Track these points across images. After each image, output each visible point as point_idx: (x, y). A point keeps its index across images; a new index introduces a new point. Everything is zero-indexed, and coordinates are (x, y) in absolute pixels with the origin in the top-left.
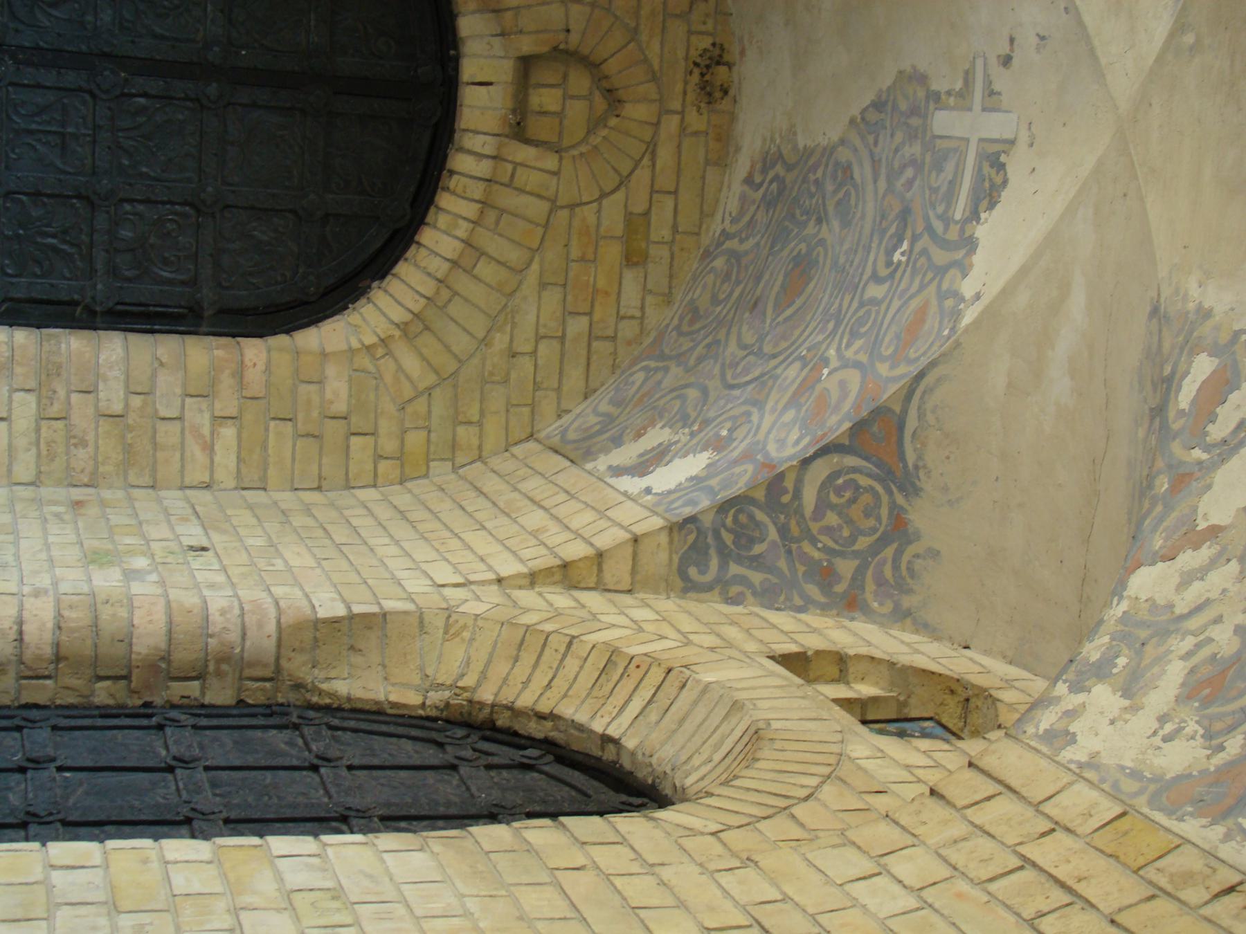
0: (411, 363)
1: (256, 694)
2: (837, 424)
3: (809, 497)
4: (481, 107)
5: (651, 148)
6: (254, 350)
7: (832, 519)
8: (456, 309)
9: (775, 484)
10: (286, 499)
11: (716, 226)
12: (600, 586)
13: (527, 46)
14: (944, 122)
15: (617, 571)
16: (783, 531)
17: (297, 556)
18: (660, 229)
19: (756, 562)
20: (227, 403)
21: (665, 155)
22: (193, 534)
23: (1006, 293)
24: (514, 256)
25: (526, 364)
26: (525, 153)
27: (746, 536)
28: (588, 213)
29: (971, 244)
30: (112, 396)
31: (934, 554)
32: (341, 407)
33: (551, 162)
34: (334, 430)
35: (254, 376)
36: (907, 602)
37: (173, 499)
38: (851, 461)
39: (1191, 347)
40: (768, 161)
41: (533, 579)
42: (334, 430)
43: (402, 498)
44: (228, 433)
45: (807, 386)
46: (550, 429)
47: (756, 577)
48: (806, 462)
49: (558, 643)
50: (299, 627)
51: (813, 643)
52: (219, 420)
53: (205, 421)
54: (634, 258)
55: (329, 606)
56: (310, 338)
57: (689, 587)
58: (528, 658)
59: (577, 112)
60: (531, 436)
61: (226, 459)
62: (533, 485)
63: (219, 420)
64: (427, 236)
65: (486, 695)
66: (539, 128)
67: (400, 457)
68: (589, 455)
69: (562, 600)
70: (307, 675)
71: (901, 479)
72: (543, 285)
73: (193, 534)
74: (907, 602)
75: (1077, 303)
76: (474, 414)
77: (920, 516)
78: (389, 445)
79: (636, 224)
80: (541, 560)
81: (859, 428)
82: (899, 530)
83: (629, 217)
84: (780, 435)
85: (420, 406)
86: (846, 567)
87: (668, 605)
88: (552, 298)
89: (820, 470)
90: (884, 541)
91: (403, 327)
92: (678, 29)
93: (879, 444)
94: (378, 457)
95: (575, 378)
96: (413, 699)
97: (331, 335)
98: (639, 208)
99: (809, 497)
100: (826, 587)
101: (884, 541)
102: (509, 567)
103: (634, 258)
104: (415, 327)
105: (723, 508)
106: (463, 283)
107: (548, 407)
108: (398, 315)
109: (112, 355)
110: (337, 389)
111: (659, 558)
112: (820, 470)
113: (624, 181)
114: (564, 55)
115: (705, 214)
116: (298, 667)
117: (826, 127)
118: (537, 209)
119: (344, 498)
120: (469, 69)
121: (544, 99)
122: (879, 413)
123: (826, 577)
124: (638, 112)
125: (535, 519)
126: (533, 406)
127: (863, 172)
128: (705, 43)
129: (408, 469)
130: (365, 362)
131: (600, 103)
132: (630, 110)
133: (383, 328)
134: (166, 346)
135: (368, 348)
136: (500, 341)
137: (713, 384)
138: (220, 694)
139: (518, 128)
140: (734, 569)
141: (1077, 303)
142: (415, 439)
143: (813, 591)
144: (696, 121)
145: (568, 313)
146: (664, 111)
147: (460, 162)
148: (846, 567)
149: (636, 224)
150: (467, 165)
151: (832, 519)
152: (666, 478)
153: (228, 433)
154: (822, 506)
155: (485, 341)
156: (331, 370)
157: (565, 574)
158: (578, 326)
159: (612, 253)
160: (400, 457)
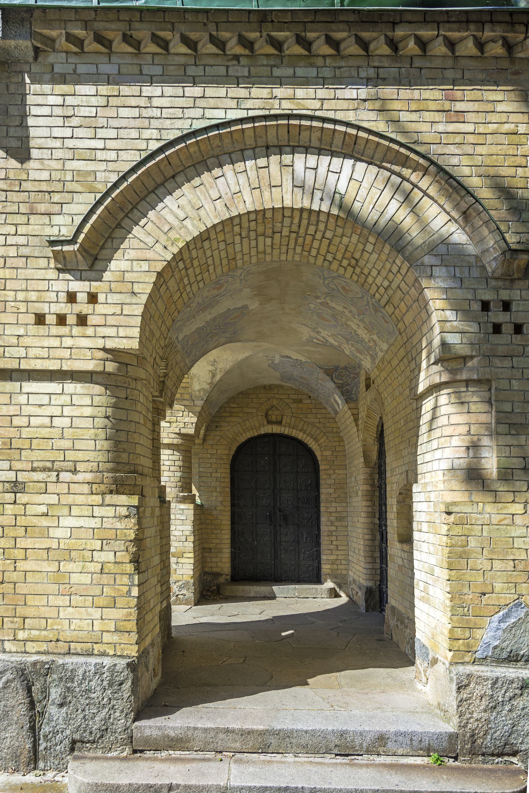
0: (322, 440)
1: (377, 471)
2: (328, 378)
3: (340, 382)
4: (276, 429)
5: (281, 399)
6: (322, 467)
7: (344, 378)
8: (312, 433)
9: (338, 387)
10: (347, 462)
11: (294, 386)
12: (358, 414)
13: (265, 422)
14: (277, 361)
15: (355, 412)
16: (347, 385)
17: (356, 462)
18: (296, 397)
19: (352, 389)
20: (331, 472)
21: (282, 397)
22: (353, 478)
23: (304, 356)
24: (302, 423)
25: (321, 420)
26: (284, 422)
27: (348, 391)
28: (293, 410)
29: (296, 359)
30: (331, 491)
31: (348, 363)
32: (331, 452)
33: (285, 417)
34: (335, 454)
35: (327, 467)
36: (357, 366)
37: (348, 481)
38: (334, 376)
39: (312, 341)
40: (282, 381)
41: (357, 425)
42: (335, 454)
43: (346, 442)
44: (336, 471)
45: (322, 380)
46: (333, 415)
47: (355, 389)
48: (335, 383)
49: (366, 424)
50: (365, 464)
51: (364, 383)
52: (334, 473)
53: (335, 475)
54: (300, 401)
55: (362, 460)
56: (319, 458)
57: (357, 400)
58: (369, 429)
59: (276, 412)
60: (334, 418)
61: (341, 472)
62: (343, 420)
63: (334, 473)
64: (299, 438)
65: (375, 435)
66: (279, 418)
67: (339, 441)
68: (337, 411)
69: (360, 422)
70: (373, 463)
71: (336, 368)
72: (307, 418)
73: (353, 478)
74: (357, 366)
75: (306, 348)
76: (331, 429)
77: (342, 365)
78: (337, 444)
79: (295, 401)
80: (353, 424)
81: (328, 375)
82: (345, 368)
83: (294, 403)
84: (331, 385)
85: (330, 438)
86: (352, 375)
87: (360, 404)
88: (309, 416)
89: (336, 381)
90: (347, 371)
91: (316, 442)
92: (260, 396)
93: (331, 372)
94: (340, 445)
95: (323, 411)
96: (376, 447)
97: (318, 454)
98: (292, 401)
99: (340, 382)
100: (355, 378)
101: (347, 371)
102: (355, 429)
103: (300, 401)
104: (316, 440)
105: (343, 395)
106: (308, 431)
107: (329, 416)
108: (314, 442)
109: (325, 492)
110: (328, 453)
111: (352, 405)
112: (336, 381)
113: (287, 404)
114: (266, 415)
115: (293, 389)
116: (372, 465)
117: (278, 374)
118: (293, 419)
119: (347, 452)
120: (270, 432)
121: (274, 418)
122: (325, 372)
123: (354, 378)
124: (275, 402)
125: (348, 422)
126: (329, 418)
127: (285, 370)
128: (262, 391)
129: (341, 440)
130: (322, 449)
131: (274, 408)
132: (275, 404)
133: (316, 445)
134: (322, 482)
135: (320, 448)
136: (317, 425)
137: (323, 391)
138: (377, 476)
139: (280, 423)
140: (353, 393)
141: (306, 348)
142: (336, 439)
143: (356, 380)
144: (276, 391)
145: (312, 413)
146: (274, 397)
147: (286, 433)
148: (352, 375)
149: (295, 401)
150: (286, 431)
151: (344, 378)
152: (340, 402)
153: (336, 471)
154: (342, 380)
155: (318, 427)
156: (324, 454)
157: (356, 420)
158: (314, 411)
159: (300, 405)
160: (339, 441)
